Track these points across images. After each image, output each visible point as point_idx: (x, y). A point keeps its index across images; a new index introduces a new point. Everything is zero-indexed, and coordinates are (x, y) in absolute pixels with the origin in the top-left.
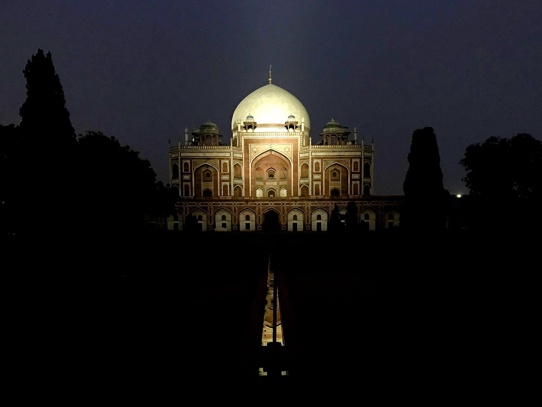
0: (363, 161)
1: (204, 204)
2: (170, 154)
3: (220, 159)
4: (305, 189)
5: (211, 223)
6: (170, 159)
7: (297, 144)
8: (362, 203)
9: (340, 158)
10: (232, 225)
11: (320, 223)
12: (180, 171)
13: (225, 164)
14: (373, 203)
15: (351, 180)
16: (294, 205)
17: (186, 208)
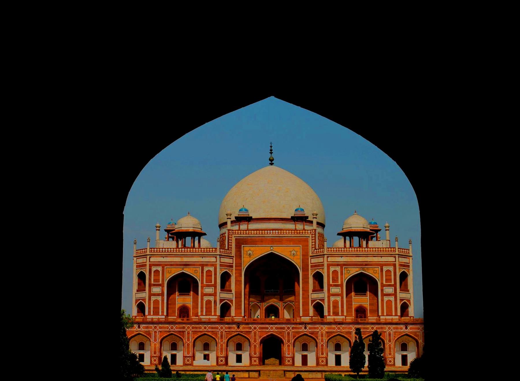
1: (180, 328)
2: (135, 259)
3: (203, 266)
5: (188, 353)
6: (135, 265)
7: (308, 246)
8: (397, 328)
9: (366, 265)
10: (217, 358)
13: (209, 271)
15: (383, 295)
16: (302, 330)
17: (155, 332)
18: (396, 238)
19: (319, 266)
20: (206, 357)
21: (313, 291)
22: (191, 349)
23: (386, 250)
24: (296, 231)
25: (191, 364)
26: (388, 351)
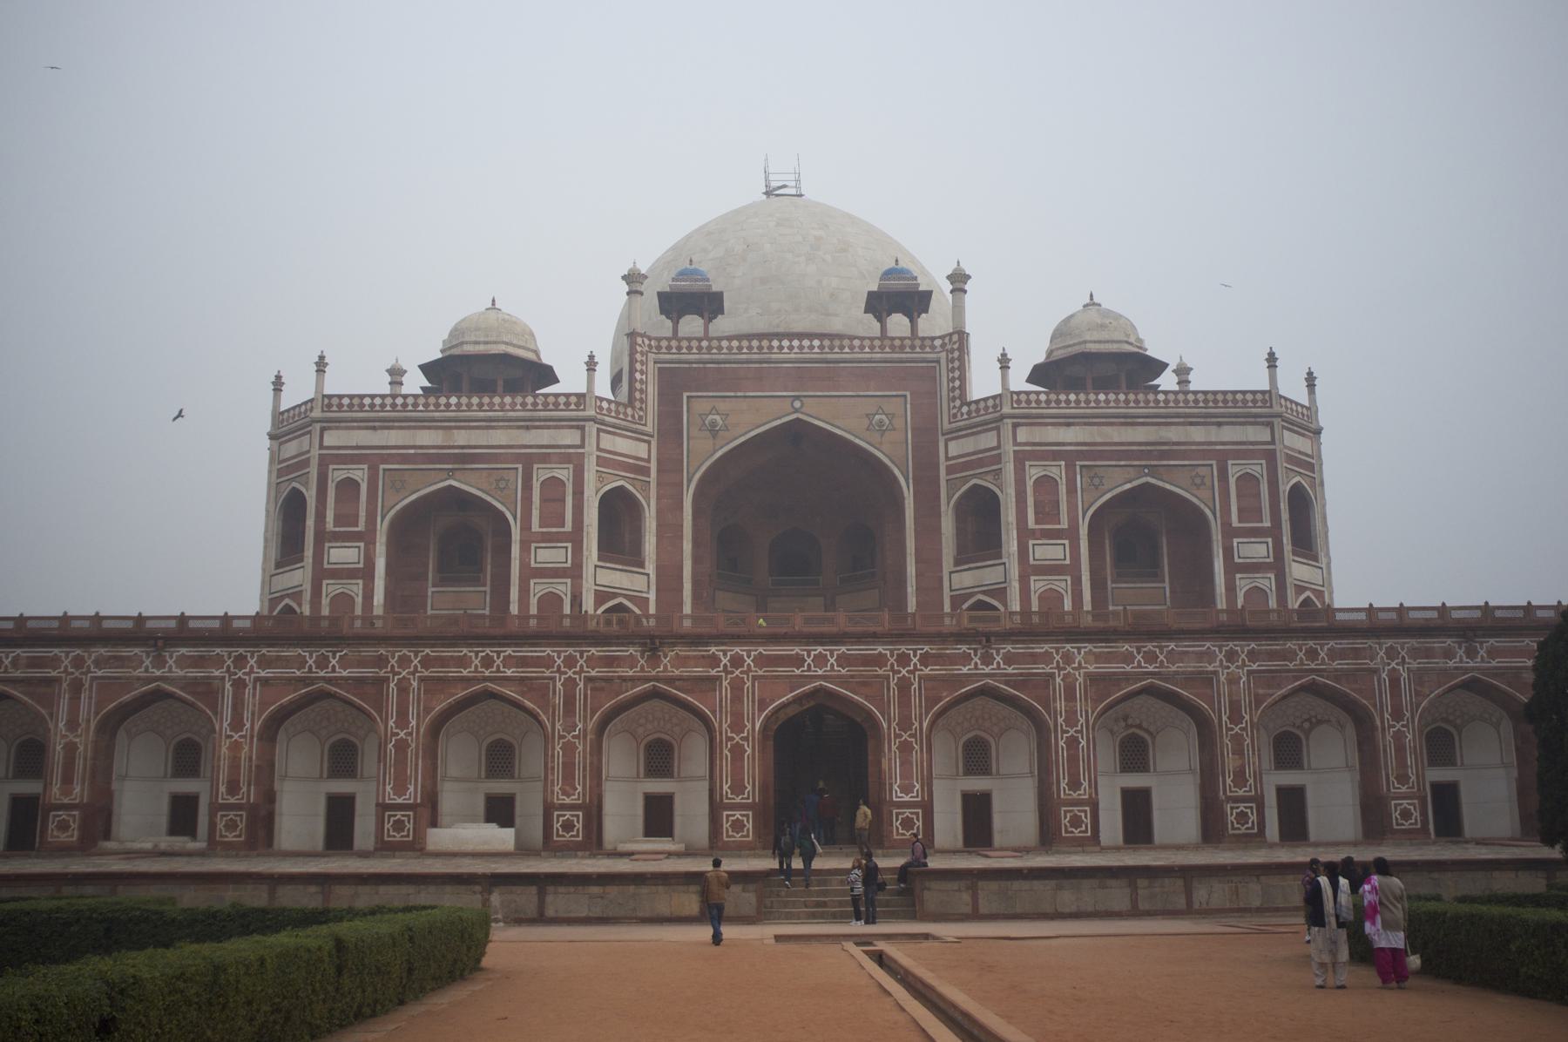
1: (362, 663)
2: (276, 443)
3: (528, 461)
5: (400, 789)
8: (1428, 653)
12: (310, 522)
13: (553, 484)
14: (1492, 653)
15: (1232, 568)
16: (977, 667)
17: (239, 685)
18: (1272, 360)
19: (980, 463)
20: (500, 811)
21: (957, 562)
23: (1235, 401)
24: (887, 342)
25: (416, 847)
26: (1392, 762)
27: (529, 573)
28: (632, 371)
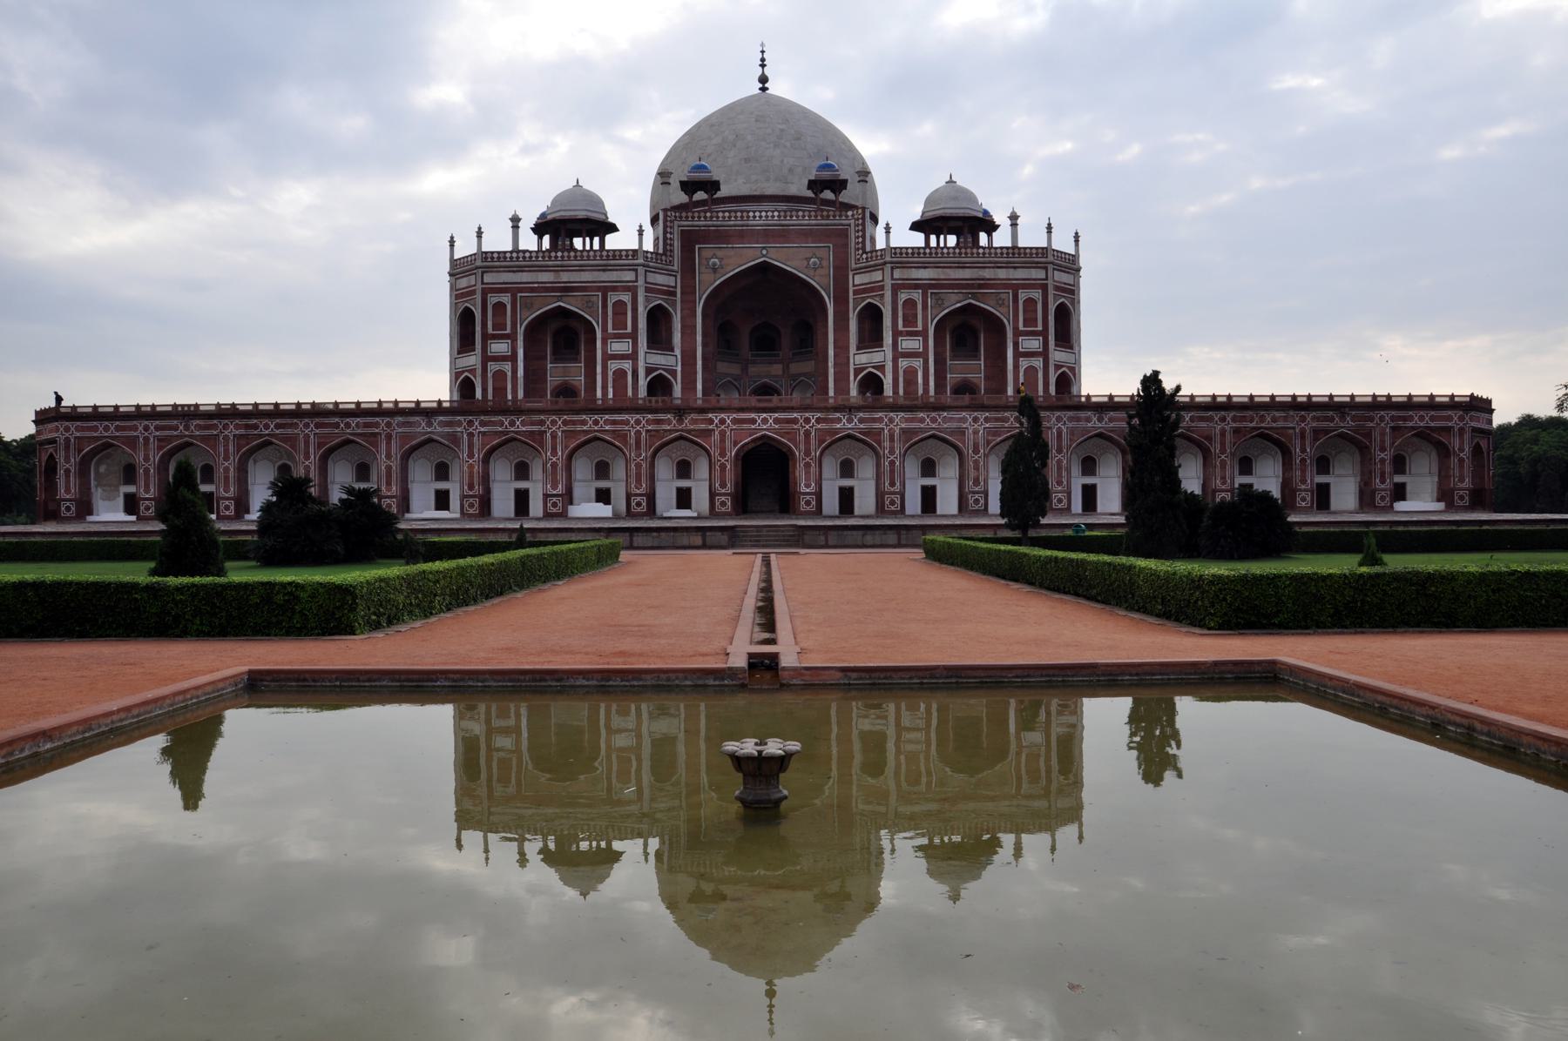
0: (1051, 298)
1: (533, 424)
3: (605, 291)
4: (872, 383)
5: (554, 487)
7: (846, 245)
8: (1078, 419)
9: (981, 286)
10: (629, 497)
11: (933, 488)
12: (478, 328)
13: (620, 305)
14: (1111, 420)
15: (1018, 355)
16: (845, 424)
17: (471, 435)
19: (872, 290)
20: (603, 496)
21: (858, 348)
22: (561, 476)
25: (563, 515)
27: (607, 357)
28: (665, 239)
